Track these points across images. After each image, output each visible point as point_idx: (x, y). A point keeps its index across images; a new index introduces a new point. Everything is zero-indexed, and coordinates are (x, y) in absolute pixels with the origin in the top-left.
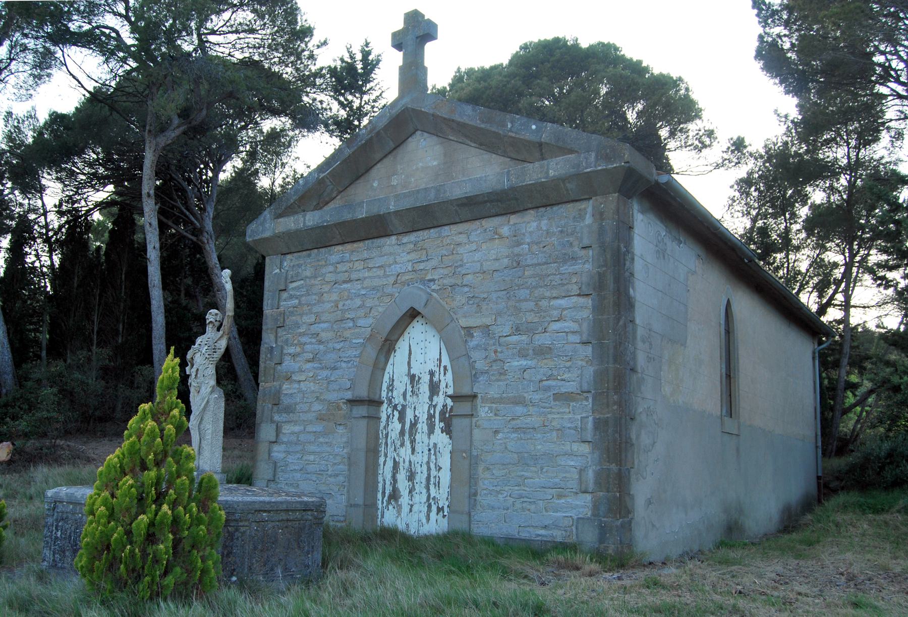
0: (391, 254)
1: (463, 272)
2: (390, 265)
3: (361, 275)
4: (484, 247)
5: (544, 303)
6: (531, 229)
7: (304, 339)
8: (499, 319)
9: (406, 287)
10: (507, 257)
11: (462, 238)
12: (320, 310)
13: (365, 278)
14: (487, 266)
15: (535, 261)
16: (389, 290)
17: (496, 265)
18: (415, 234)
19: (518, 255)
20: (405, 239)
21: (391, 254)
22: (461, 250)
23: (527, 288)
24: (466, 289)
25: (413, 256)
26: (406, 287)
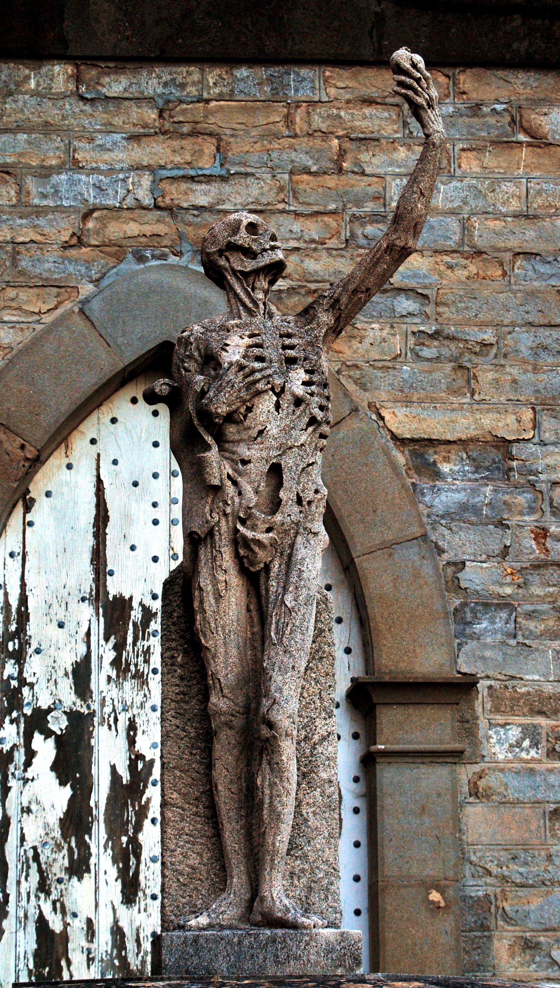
0: (47, 129)
2: (45, 173)
8: (548, 423)
14: (484, 232)
16: (48, 264)
18: (165, 73)
20: (116, 85)
21: (47, 129)
25: (158, 151)
26: (130, 265)
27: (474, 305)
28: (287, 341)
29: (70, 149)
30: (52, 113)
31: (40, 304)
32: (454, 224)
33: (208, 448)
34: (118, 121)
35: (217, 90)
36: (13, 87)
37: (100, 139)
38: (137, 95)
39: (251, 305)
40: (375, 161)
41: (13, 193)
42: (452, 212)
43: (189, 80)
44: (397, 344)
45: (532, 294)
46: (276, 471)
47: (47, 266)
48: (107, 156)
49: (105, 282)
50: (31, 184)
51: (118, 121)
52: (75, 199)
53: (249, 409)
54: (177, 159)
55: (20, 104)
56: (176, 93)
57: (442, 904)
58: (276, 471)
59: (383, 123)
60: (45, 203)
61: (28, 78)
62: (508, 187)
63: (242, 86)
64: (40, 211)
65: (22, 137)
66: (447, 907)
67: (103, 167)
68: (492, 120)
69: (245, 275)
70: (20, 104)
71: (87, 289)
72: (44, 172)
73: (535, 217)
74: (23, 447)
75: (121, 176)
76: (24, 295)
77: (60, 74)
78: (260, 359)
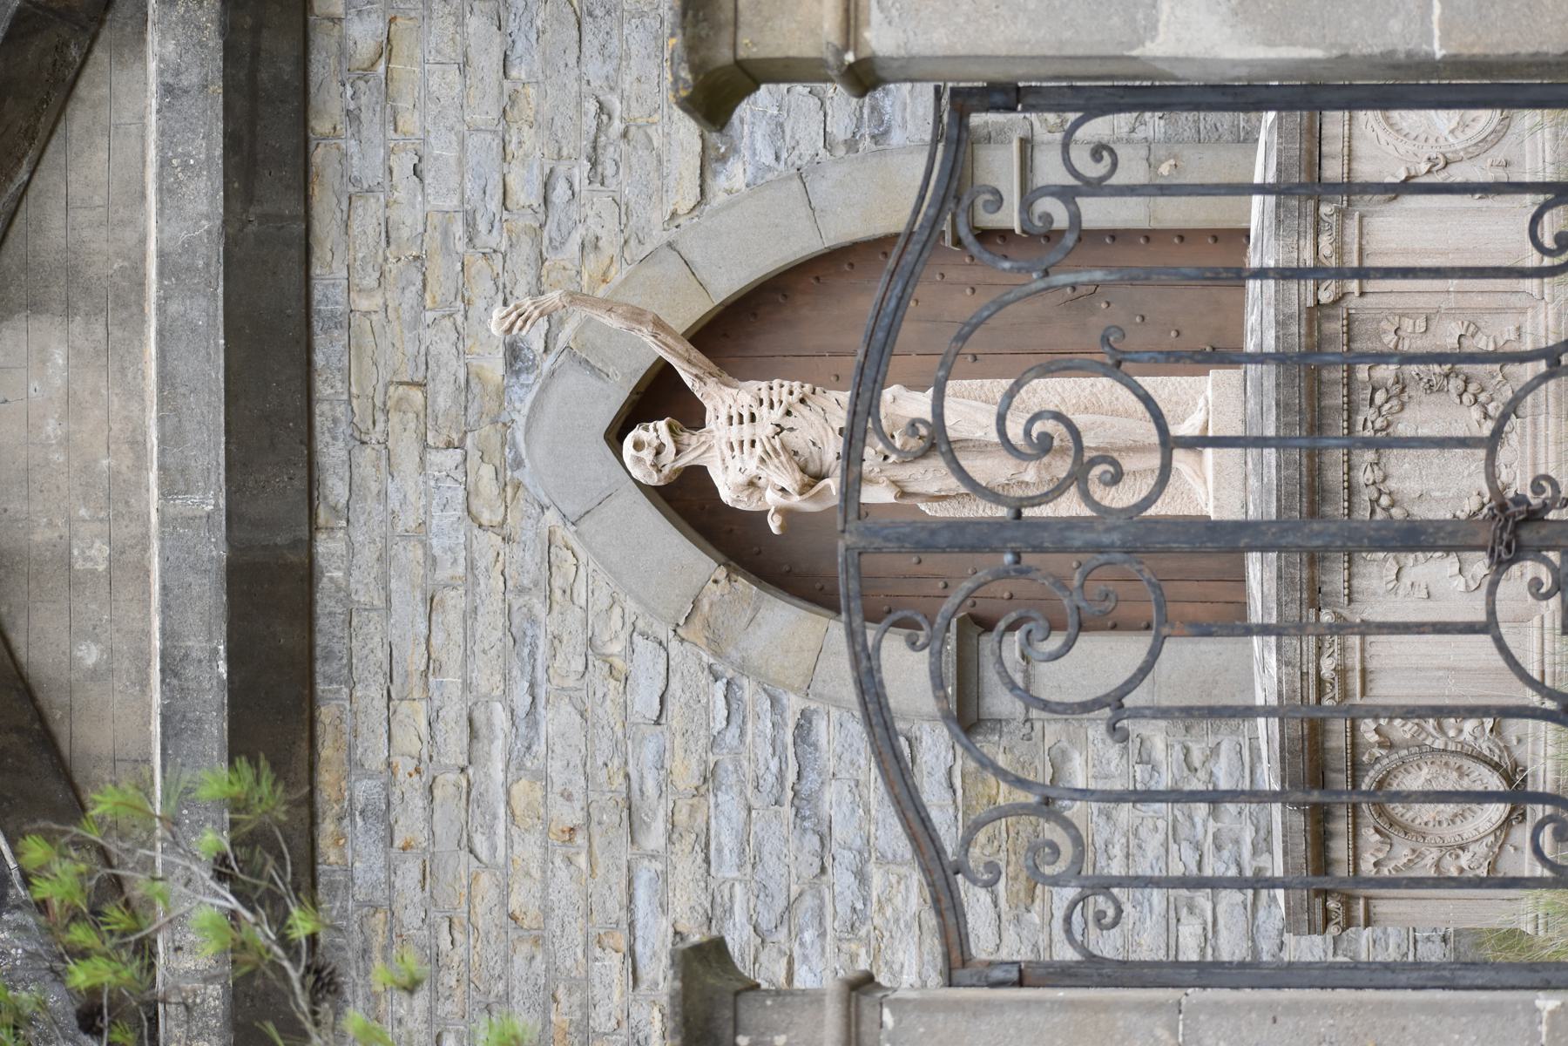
1: (494, 205)
2: (432, 562)
3: (453, 712)
4: (410, 121)
9: (524, 475)
10: (460, 22)
11: (367, 218)
12: (576, 932)
13: (467, 686)
14: (485, 112)
16: (527, 560)
17: (487, 63)
18: (322, 438)
20: (335, 488)
22: (408, 219)
24: (560, 192)
25: (406, 450)
26: (524, 475)
27: (558, 123)
28: (736, 419)
30: (367, 555)
31: (567, 565)
32: (474, 141)
33: (828, 487)
34: (374, 487)
35: (339, 385)
36: (342, 594)
37: (394, 503)
38: (347, 467)
39: (704, 448)
40: (409, 222)
41: (453, 593)
42: (462, 143)
43: (329, 414)
44: (603, 201)
45: (546, 61)
47: (527, 557)
48: (412, 497)
49: (546, 501)
50: (443, 574)
51: (374, 487)
52: (457, 530)
53: (796, 453)
54: (412, 425)
55: (359, 586)
56: (343, 426)
57: (1172, 162)
59: (370, 213)
60: (462, 561)
61: (331, 579)
62: (434, 82)
63: (334, 360)
64: (471, 566)
65: (393, 585)
66: (1175, 157)
67: (423, 502)
68: (364, 100)
69: (678, 452)
70: (359, 586)
71: (551, 517)
72: (429, 562)
73: (466, 55)
74: (716, 582)
75: (432, 483)
76: (557, 583)
77: (328, 547)
78: (753, 443)
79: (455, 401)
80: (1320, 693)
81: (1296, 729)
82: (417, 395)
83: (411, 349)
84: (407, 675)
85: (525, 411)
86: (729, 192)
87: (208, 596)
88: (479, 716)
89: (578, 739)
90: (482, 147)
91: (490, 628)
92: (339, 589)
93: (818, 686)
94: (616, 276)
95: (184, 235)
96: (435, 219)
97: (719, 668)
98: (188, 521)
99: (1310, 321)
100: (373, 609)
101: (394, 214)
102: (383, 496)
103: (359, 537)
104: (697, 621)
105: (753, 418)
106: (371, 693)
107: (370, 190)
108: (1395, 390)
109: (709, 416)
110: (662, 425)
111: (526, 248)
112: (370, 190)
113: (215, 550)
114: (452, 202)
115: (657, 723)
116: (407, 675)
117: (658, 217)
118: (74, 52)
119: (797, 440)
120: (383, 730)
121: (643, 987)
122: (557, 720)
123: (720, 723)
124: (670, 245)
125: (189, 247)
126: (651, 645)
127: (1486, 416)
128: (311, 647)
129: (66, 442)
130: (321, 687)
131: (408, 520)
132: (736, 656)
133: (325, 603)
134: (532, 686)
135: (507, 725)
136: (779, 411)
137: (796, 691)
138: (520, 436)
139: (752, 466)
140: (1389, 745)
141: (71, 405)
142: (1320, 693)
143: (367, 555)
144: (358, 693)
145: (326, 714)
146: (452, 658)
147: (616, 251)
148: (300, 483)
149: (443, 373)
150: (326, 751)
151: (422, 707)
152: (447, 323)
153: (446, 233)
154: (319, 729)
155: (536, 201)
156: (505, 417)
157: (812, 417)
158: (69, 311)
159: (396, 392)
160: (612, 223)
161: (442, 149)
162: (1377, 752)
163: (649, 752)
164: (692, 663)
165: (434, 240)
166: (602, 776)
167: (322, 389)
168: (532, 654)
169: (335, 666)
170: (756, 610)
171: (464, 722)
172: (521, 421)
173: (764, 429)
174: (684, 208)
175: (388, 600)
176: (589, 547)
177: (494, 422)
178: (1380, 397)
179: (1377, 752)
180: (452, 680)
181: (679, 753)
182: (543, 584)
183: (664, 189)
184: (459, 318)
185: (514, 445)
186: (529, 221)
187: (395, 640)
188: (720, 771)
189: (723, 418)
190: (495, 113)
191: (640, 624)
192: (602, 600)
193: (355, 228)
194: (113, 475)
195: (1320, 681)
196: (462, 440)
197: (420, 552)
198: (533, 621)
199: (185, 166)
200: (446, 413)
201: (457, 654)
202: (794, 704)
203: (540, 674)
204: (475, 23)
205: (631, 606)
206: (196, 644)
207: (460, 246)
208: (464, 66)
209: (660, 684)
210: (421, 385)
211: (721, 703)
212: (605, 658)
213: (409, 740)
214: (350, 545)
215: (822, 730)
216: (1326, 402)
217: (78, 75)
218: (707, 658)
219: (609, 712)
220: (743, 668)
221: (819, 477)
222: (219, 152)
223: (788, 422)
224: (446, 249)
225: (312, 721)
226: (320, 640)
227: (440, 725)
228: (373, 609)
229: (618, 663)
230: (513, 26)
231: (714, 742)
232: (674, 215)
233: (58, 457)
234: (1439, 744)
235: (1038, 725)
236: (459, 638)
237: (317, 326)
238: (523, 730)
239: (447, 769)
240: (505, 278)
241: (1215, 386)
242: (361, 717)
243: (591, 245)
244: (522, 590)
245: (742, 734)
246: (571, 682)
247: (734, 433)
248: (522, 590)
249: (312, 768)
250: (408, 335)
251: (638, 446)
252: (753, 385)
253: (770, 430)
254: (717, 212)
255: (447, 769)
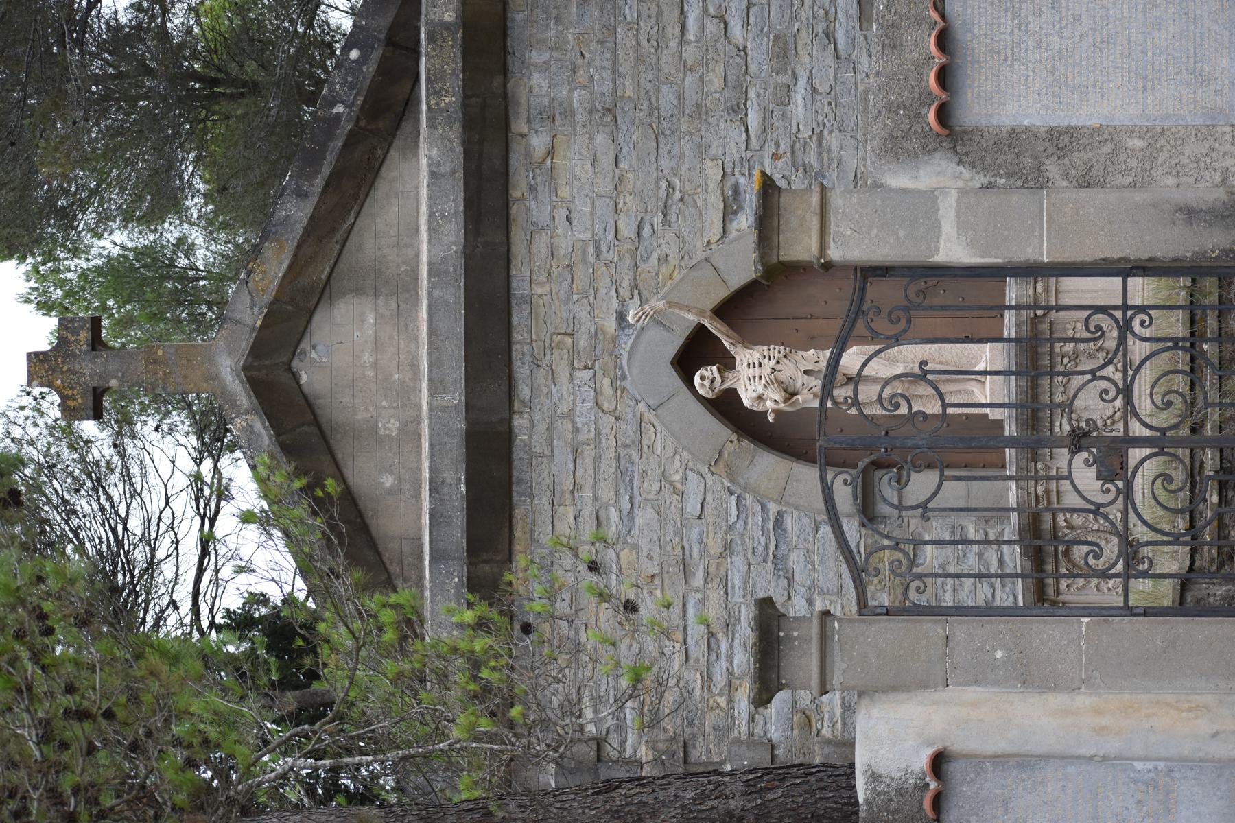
1: (611, 237)
2: (577, 430)
3: (588, 512)
4: (564, 191)
5: (691, 53)
6: (544, 84)
7: (719, 677)
8: (713, 151)
9: (627, 384)
10: (592, 138)
11: (541, 244)
14: (605, 187)
15: (607, 74)
16: (630, 429)
17: (607, 160)
18: (516, 364)
19: (591, 112)
20: (524, 391)
21: (550, 429)
23: (658, 90)
24: (647, 230)
26: (627, 384)
27: (645, 192)
29: (562, 417)
30: (541, 427)
32: (599, 202)
34: (545, 390)
37: (556, 399)
42: (593, 203)
45: (638, 159)
46: (806, 372)
48: (566, 396)
49: (639, 398)
50: (582, 438)
51: (545, 390)
54: (566, 357)
58: (806, 372)
62: (578, 170)
63: (523, 321)
64: (598, 432)
65: (555, 443)
68: (539, 179)
71: (642, 407)
73: (595, 155)
76: (645, 442)
77: (519, 422)
79: (589, 343)
80: (1037, 503)
81: (1026, 519)
82: (568, 340)
83: (565, 315)
84: (563, 492)
85: (628, 349)
86: (739, 231)
87: (455, 449)
88: (602, 514)
89: (656, 527)
90: (604, 205)
91: (608, 467)
92: (525, 445)
93: (786, 498)
94: (677, 276)
95: (442, 254)
96: (579, 245)
97: (733, 488)
98: (445, 409)
99: (1032, 324)
100: (544, 456)
101: (556, 242)
102: (549, 395)
103: (536, 417)
104: (721, 464)
105: (760, 365)
106: (543, 502)
107: (542, 229)
108: (1073, 357)
109: (738, 363)
110: (714, 368)
111: (628, 261)
112: (542, 229)
113: (459, 424)
114: (588, 235)
115: (699, 518)
116: (563, 492)
117: (700, 244)
118: (379, 152)
119: (783, 376)
120: (549, 522)
121: (691, 661)
122: (644, 517)
123: (733, 518)
124: (706, 259)
125: (445, 260)
126: (696, 476)
127: (1117, 370)
128: (510, 477)
129: (375, 365)
130: (515, 498)
131: (564, 408)
132: (742, 482)
133: (518, 453)
134: (631, 498)
135: (617, 519)
136: (773, 362)
137: (775, 501)
138: (625, 363)
139: (760, 389)
140: (1071, 527)
141: (378, 345)
142: (1037, 503)
143: (541, 427)
144: (536, 502)
145: (518, 513)
146: (587, 483)
147: (677, 263)
148: (505, 388)
149: (583, 329)
150: (518, 534)
151: (571, 509)
152: (585, 301)
153: (584, 252)
154: (514, 521)
155: (633, 235)
156: (616, 352)
157: (790, 365)
158: (376, 293)
159: (556, 339)
160: (675, 248)
161: (582, 206)
162: (1066, 531)
163: (695, 534)
164: (718, 484)
165: (577, 256)
166: (669, 547)
167: (517, 337)
168: (631, 481)
169: (523, 487)
170: (753, 457)
171: (594, 517)
172: (625, 354)
173: (766, 371)
174: (714, 240)
175: (553, 451)
176: (663, 423)
177: (611, 355)
178: (1066, 360)
179: (1066, 531)
180: (587, 495)
181: (711, 534)
182: (637, 442)
183: (703, 229)
184: (592, 299)
185: (621, 368)
186: (629, 246)
187: (557, 473)
188: (733, 545)
189: (745, 365)
190: (611, 188)
191: (690, 464)
192: (670, 452)
193: (534, 250)
194: (401, 383)
195: (1037, 497)
196: (593, 365)
197: (570, 426)
198: (632, 462)
199: (443, 216)
200: (584, 349)
201: (590, 481)
202: (773, 508)
203: (635, 492)
204: (600, 138)
205: (685, 454)
206: (449, 475)
207: (592, 260)
208: (594, 161)
209: (701, 497)
210: (571, 335)
211: (734, 507)
212: (671, 483)
213: (564, 528)
214: (532, 421)
215: (788, 521)
216: (1040, 363)
217: (381, 165)
218: (726, 483)
219: (673, 512)
220: (746, 489)
221: (794, 394)
222: (461, 209)
223: (778, 367)
224: (584, 261)
225: (511, 517)
226: (515, 473)
227: (581, 519)
228: (544, 456)
229: (678, 485)
230: (621, 140)
231: (730, 529)
232: (709, 243)
233: (370, 373)
234: (1095, 527)
235: (906, 520)
236: (592, 472)
237: (514, 302)
238: (626, 522)
239: (584, 543)
240: (616, 277)
241: (991, 350)
242: (537, 515)
243: (664, 259)
244: (625, 446)
245: (746, 524)
246: (652, 496)
247: (751, 372)
248: (625, 446)
249: (511, 543)
250: (563, 308)
251: (702, 378)
252: (760, 348)
253: (769, 371)
254: (731, 242)
255: (584, 543)
